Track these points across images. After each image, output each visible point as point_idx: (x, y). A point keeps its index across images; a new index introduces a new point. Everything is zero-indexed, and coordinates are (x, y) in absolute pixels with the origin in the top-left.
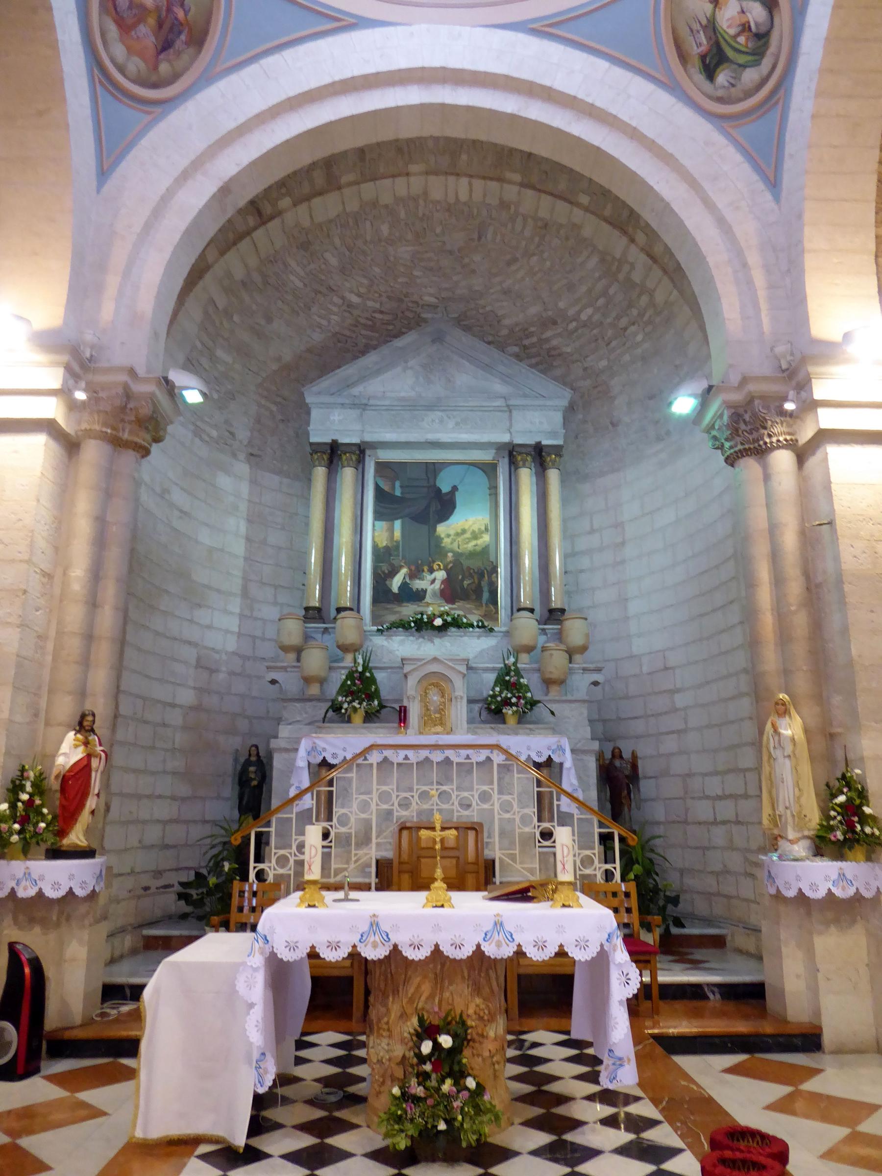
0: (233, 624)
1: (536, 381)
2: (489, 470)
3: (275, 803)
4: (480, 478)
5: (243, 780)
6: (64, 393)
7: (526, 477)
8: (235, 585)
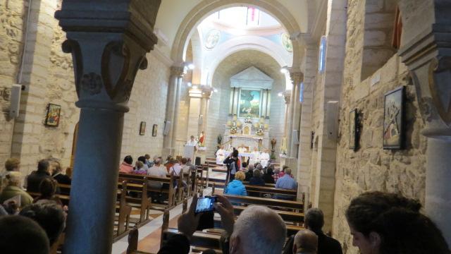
0: (218, 115)
1: (268, 78)
2: (259, 92)
4: (258, 94)
5: (218, 139)
6: (202, 94)
7: (265, 95)
8: (218, 109)
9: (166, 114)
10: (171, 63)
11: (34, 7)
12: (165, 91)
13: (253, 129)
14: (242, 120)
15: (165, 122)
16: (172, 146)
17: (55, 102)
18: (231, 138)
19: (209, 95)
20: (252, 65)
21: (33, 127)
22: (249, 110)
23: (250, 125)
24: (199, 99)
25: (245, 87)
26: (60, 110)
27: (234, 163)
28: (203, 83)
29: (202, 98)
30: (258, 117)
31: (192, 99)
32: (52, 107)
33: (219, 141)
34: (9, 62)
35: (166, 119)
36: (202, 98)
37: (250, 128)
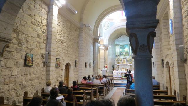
2: (128, 45)
3: (115, 68)
8: (111, 54)
9: (93, 58)
10: (93, 37)
11: (50, 22)
12: (92, 48)
13: (127, 61)
14: (121, 57)
15: (93, 61)
16: (97, 71)
17: (58, 57)
18: (118, 65)
19: (108, 48)
20: (124, 34)
21: (53, 68)
22: (124, 53)
23: (125, 59)
24: (104, 51)
25: (121, 44)
26: (60, 60)
27: (130, 76)
28: (105, 44)
29: (105, 50)
30: (128, 55)
31: (101, 51)
32: (57, 60)
33: (113, 67)
34: (43, 43)
35: (93, 60)
36: (105, 50)
37: (126, 61)
